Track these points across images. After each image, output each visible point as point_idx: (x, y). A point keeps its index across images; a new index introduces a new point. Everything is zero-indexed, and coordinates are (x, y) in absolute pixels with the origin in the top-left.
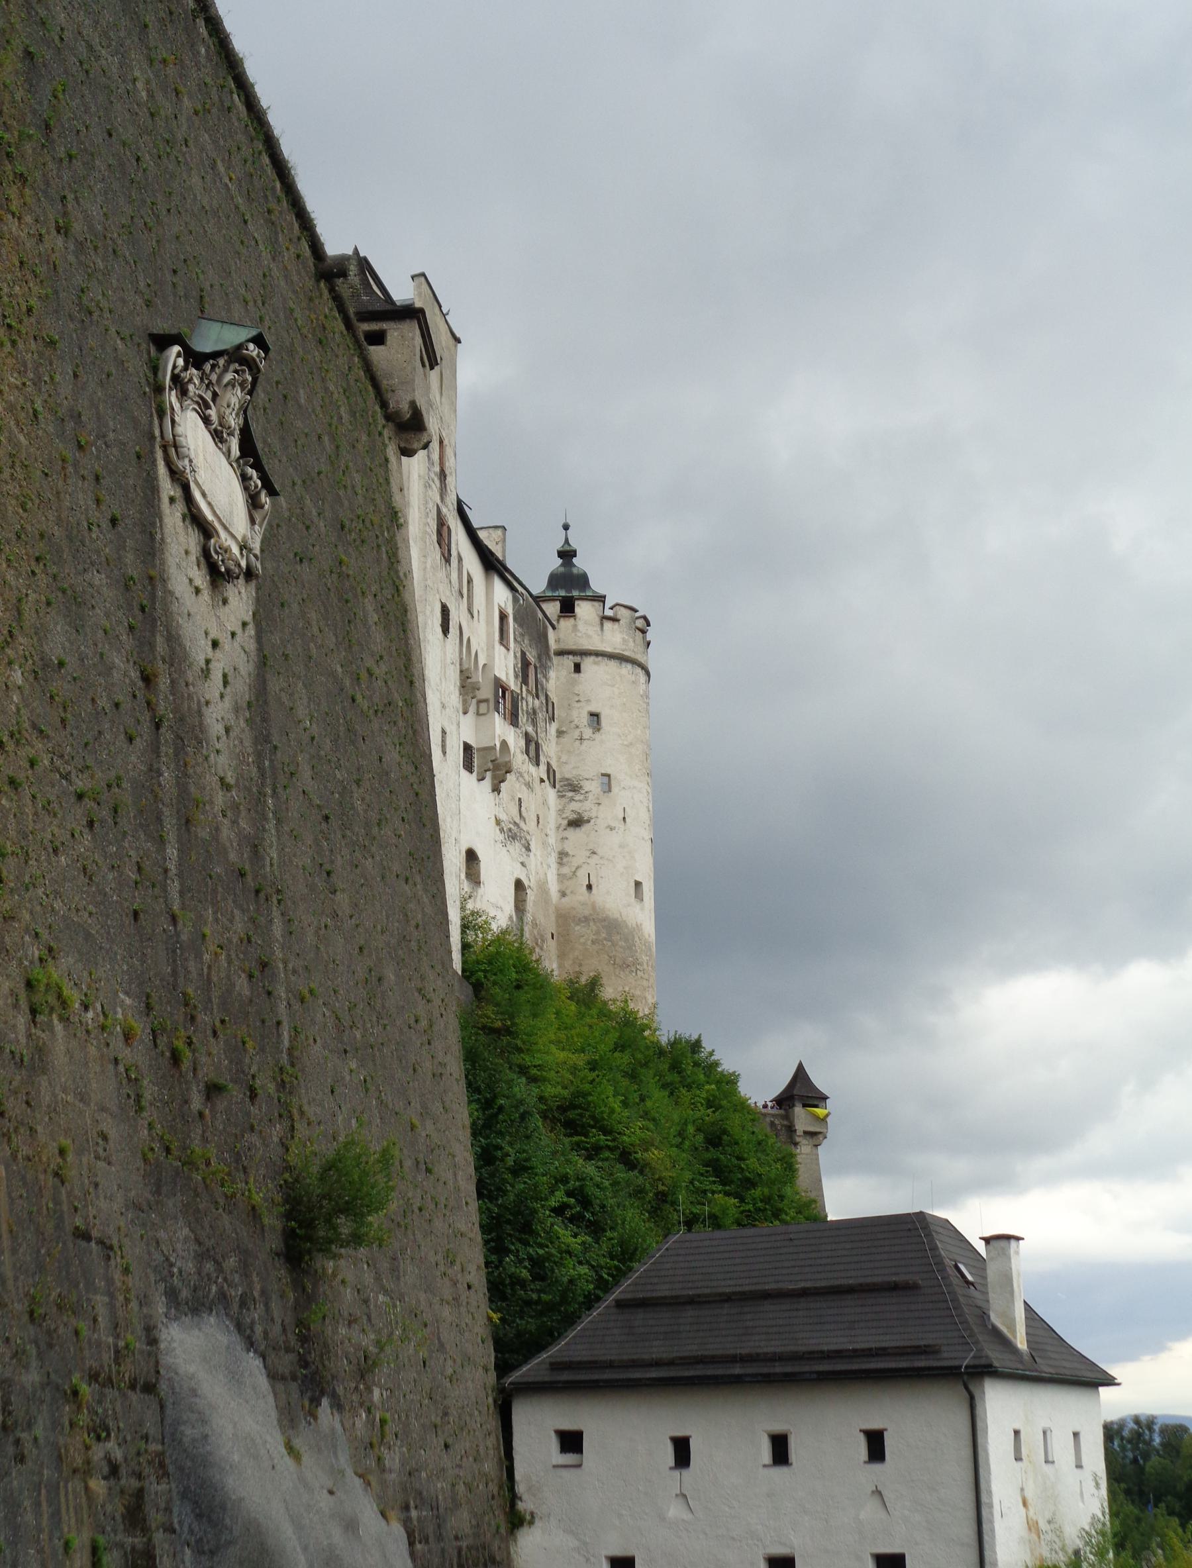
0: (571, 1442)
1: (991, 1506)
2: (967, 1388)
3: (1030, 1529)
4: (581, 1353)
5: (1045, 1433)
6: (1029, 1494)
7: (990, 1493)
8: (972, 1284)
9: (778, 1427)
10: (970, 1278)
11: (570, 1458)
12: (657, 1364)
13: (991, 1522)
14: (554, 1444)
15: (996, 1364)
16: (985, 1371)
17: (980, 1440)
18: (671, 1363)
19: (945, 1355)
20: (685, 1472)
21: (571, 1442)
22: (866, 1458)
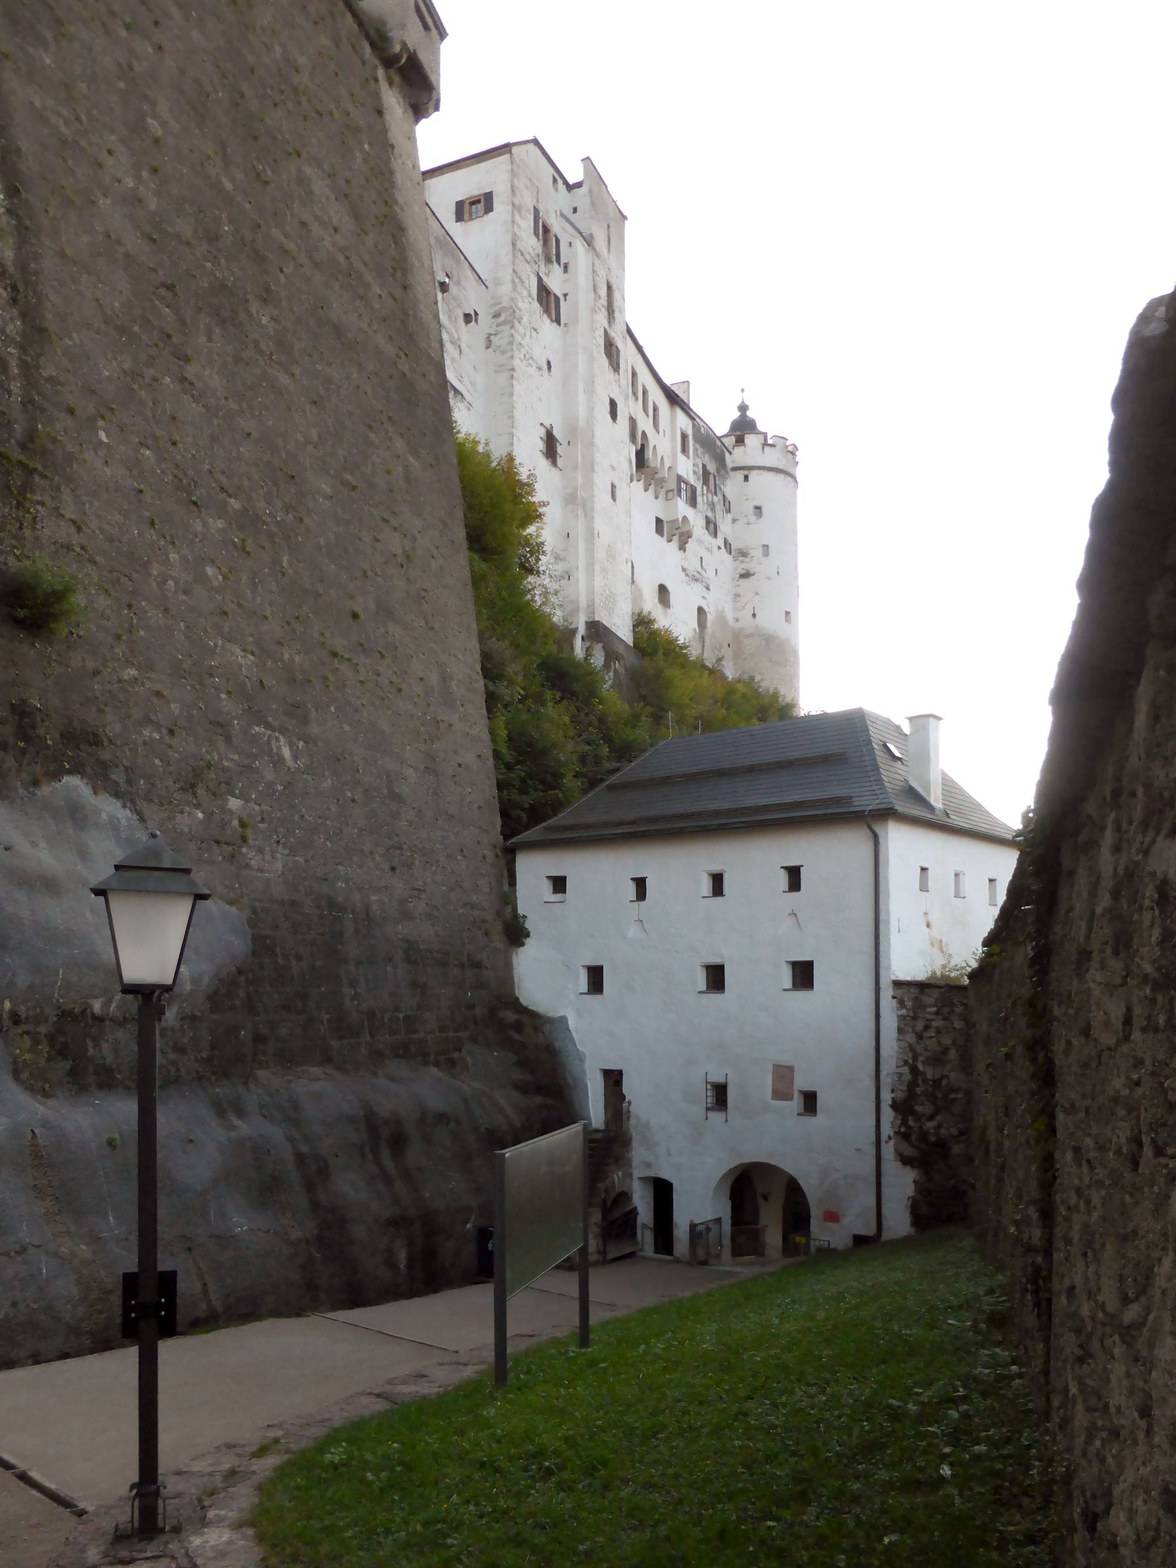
0: (559, 884)
1: (888, 923)
2: (870, 828)
3: (932, 944)
4: (570, 821)
5: (957, 875)
6: (932, 918)
7: (888, 913)
8: (899, 759)
9: (716, 868)
10: (897, 753)
11: (559, 897)
12: (620, 824)
13: (888, 935)
14: (548, 886)
15: (897, 807)
16: (887, 814)
17: (881, 871)
18: (633, 823)
19: (855, 804)
20: (641, 903)
21: (559, 884)
22: (786, 888)
